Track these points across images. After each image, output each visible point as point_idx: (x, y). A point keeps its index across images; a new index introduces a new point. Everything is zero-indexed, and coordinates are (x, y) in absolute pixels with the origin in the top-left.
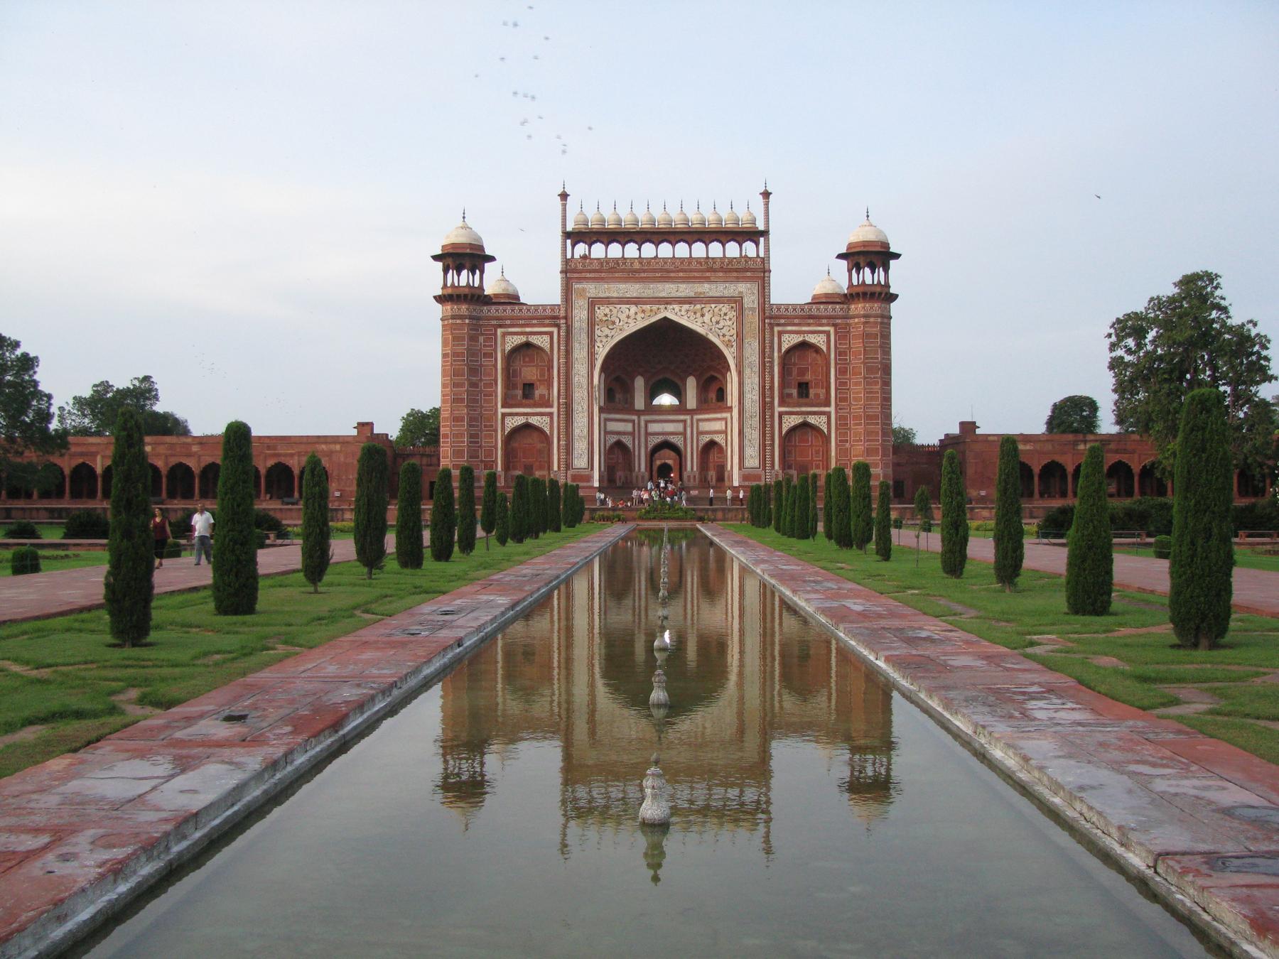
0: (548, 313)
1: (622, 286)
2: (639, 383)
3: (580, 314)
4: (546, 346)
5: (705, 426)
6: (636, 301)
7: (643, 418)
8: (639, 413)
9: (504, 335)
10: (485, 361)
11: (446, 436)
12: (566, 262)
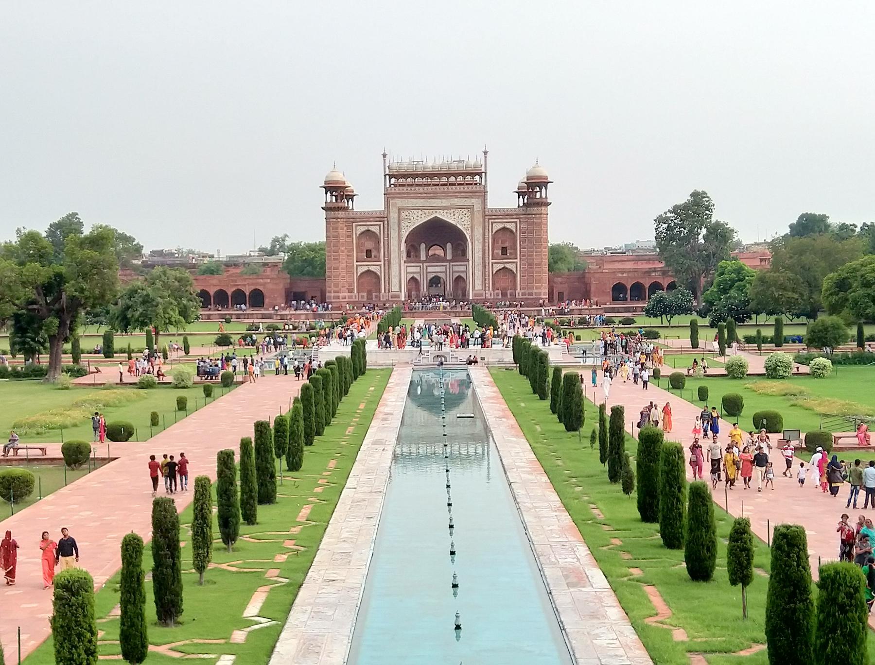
0: (378, 215)
1: (414, 201)
2: (423, 246)
3: (394, 215)
4: (377, 232)
5: (456, 269)
6: (422, 209)
7: (425, 264)
8: (423, 262)
9: (357, 226)
10: (349, 239)
11: (329, 277)
12: (386, 189)
